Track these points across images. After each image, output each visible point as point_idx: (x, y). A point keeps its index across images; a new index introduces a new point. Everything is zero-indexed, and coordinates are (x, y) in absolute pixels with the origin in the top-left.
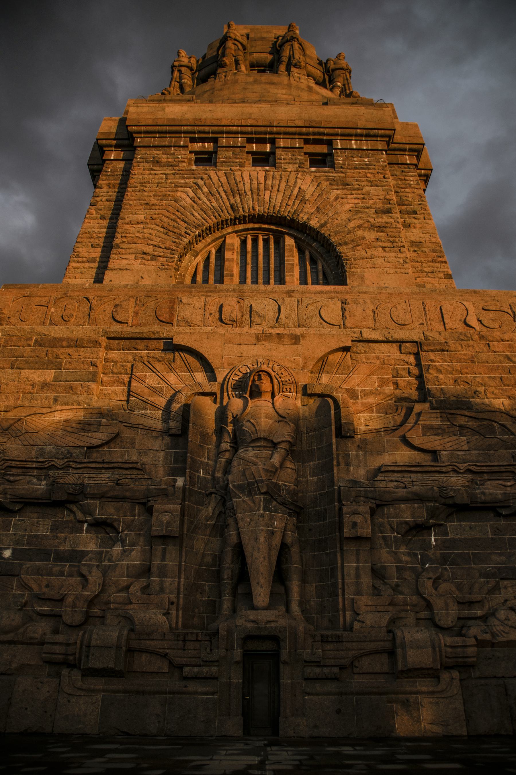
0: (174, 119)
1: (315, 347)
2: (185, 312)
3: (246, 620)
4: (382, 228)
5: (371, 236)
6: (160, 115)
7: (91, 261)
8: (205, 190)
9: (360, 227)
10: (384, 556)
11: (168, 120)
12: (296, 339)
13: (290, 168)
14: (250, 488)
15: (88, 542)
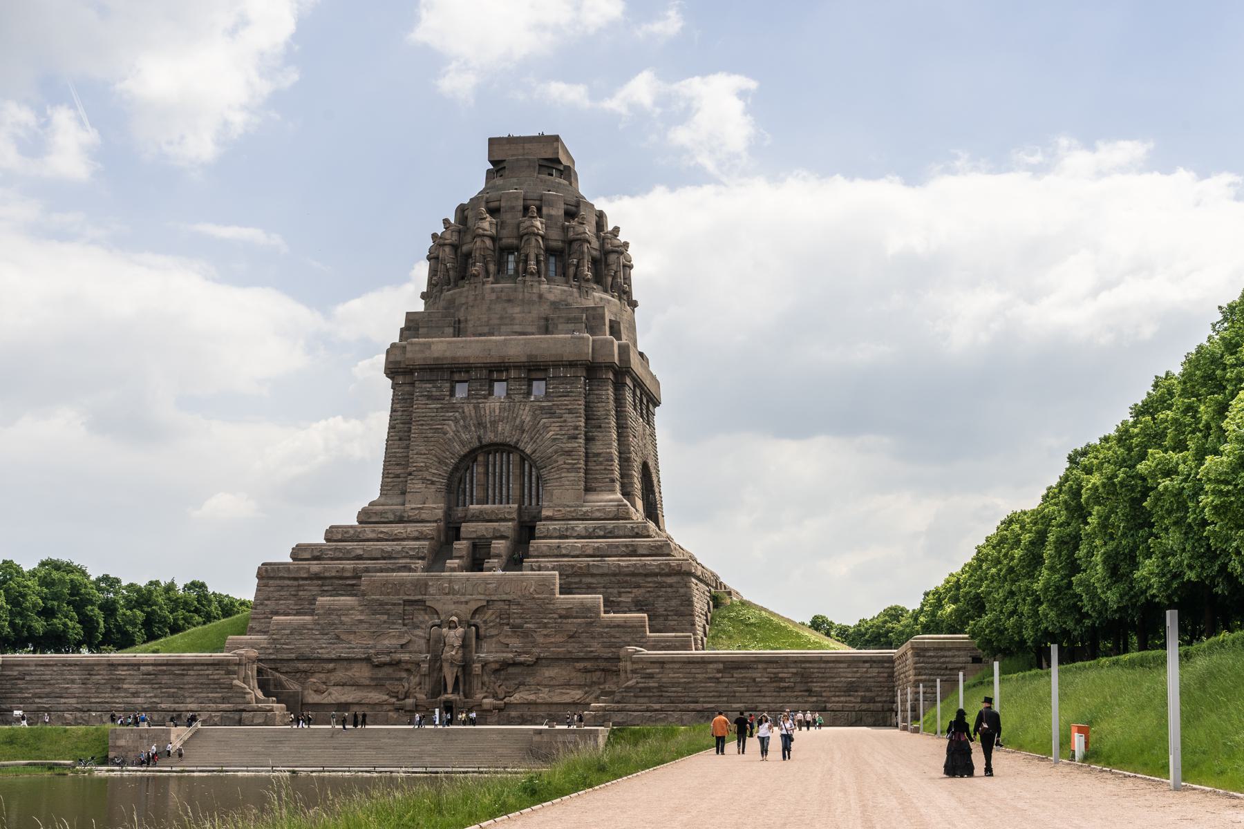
0: (438, 358)
1: (474, 606)
2: (432, 590)
3: (444, 697)
4: (568, 453)
5: (561, 460)
6: (427, 354)
7: (398, 476)
8: (462, 422)
9: (556, 452)
10: (486, 679)
11: (435, 359)
12: (467, 603)
13: (518, 398)
14: (447, 660)
15: (404, 675)
